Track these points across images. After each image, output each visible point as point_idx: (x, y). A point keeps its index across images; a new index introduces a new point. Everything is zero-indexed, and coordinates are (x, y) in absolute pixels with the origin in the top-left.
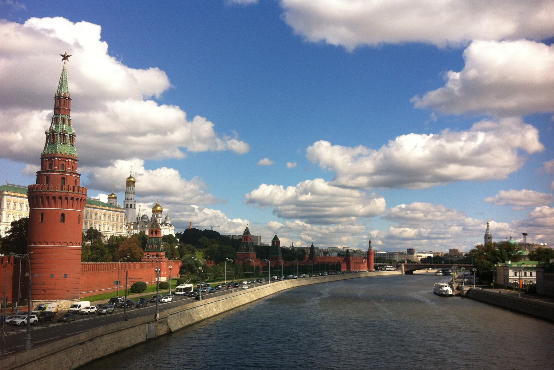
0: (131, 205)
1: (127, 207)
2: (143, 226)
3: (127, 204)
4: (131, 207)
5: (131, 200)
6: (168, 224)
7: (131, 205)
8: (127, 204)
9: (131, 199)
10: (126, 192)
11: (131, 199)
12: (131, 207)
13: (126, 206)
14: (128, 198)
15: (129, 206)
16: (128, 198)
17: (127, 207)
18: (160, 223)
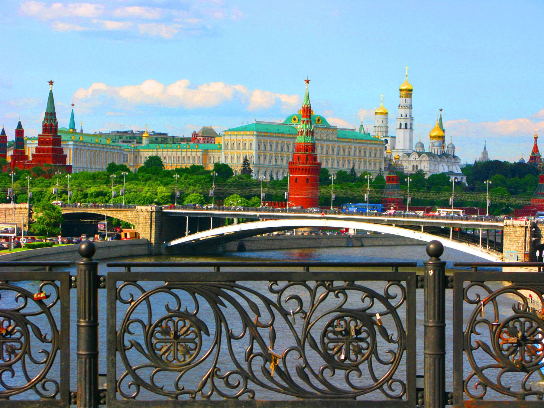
0: (406, 124)
1: (400, 128)
2: (415, 159)
3: (401, 124)
4: (406, 128)
5: (406, 118)
6: (451, 156)
7: (406, 124)
8: (401, 124)
9: (406, 116)
10: (399, 106)
11: (406, 116)
12: (406, 128)
13: (398, 127)
14: (402, 115)
15: (403, 126)
16: (402, 115)
17: (400, 128)
18: (439, 154)
